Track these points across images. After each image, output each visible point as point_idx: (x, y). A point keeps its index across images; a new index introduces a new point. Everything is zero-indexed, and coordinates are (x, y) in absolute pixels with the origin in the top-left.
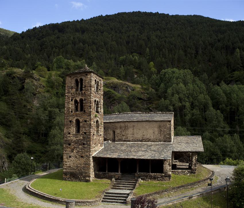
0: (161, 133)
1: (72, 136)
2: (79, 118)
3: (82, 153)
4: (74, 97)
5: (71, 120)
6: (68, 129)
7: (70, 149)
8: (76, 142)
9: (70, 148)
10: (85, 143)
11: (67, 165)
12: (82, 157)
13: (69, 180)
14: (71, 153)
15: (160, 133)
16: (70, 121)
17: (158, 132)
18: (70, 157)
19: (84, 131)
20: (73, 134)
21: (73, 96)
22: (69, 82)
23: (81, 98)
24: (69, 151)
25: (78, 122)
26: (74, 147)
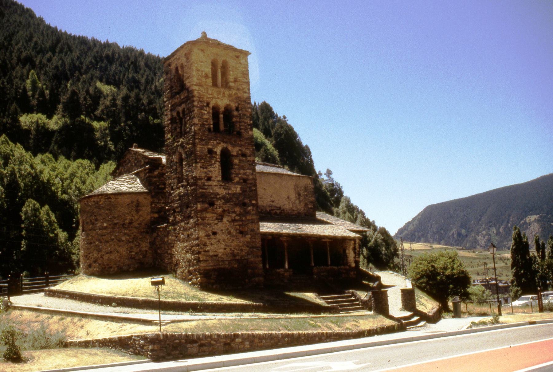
0: (299, 199)
1: (216, 186)
2: (230, 148)
3: (241, 223)
4: (213, 98)
5: (210, 147)
6: (206, 168)
7: (213, 215)
8: (227, 200)
10: (247, 201)
11: (208, 251)
12: (241, 232)
14: (216, 224)
15: (299, 199)
17: (296, 197)
18: (215, 233)
20: (218, 181)
21: (210, 94)
23: (228, 102)
24: (211, 219)
25: (226, 156)
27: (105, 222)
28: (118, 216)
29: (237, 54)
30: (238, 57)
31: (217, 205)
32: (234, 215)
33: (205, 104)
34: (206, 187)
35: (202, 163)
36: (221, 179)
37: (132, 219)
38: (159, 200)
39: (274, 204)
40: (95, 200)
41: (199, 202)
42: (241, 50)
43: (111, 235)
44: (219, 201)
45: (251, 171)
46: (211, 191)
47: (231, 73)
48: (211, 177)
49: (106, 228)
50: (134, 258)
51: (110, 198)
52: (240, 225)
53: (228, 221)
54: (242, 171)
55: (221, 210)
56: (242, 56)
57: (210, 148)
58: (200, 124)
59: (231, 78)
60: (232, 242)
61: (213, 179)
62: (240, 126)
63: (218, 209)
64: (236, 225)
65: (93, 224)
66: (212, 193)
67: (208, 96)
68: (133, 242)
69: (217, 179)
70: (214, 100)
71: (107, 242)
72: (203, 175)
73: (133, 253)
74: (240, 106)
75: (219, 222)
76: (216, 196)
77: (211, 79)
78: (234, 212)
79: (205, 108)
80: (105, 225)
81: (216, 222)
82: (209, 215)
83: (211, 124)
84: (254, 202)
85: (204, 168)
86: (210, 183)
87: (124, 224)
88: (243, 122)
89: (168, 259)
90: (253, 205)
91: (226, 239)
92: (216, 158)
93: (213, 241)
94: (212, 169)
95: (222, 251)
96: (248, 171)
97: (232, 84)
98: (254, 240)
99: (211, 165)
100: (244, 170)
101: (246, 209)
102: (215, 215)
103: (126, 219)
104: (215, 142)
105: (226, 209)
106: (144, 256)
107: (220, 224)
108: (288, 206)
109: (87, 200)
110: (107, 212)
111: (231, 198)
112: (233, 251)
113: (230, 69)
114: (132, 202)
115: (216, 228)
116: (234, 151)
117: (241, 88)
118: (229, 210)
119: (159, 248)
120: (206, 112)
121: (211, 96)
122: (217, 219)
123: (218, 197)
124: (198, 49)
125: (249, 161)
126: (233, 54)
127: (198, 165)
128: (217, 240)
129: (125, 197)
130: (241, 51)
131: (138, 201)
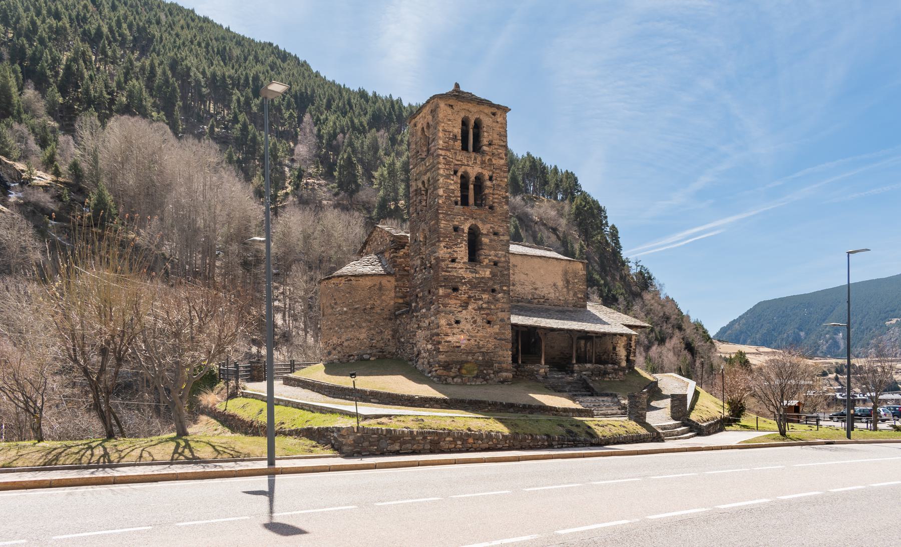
0: (568, 286)
2: (480, 225)
3: (489, 312)
4: (462, 165)
6: (451, 248)
8: (473, 285)
9: (456, 298)
10: (497, 287)
12: (489, 322)
13: (457, 384)
14: (459, 312)
15: (567, 287)
16: (456, 229)
17: (564, 285)
18: (457, 322)
19: (494, 258)
20: (464, 263)
22: (449, 120)
23: (480, 170)
24: (454, 306)
26: (468, 298)
27: (345, 307)
28: (358, 301)
29: (494, 110)
30: (494, 114)
31: (461, 290)
32: (481, 302)
33: (452, 173)
34: (450, 270)
35: (446, 241)
36: (467, 261)
37: (374, 304)
38: (404, 284)
39: (537, 292)
40: (335, 282)
41: (441, 286)
42: (498, 105)
43: (351, 321)
44: (464, 286)
45: (504, 253)
46: (455, 274)
47: (485, 134)
48: (457, 258)
49: (346, 312)
50: (375, 346)
51: (351, 280)
52: (487, 314)
53: (473, 309)
54: (492, 253)
55: (466, 296)
56: (499, 113)
57: (455, 225)
58: (446, 196)
59: (485, 141)
60: (477, 333)
61: (457, 260)
62: (493, 198)
63: (463, 295)
64: (483, 314)
65: (333, 308)
66: (458, 277)
67: (457, 163)
68: (374, 329)
69: (462, 261)
70: (463, 167)
71: (347, 328)
72: (448, 256)
73: (374, 341)
74: (494, 175)
75: (463, 309)
76: (462, 280)
77: (460, 141)
78: (481, 299)
79: (452, 177)
80: (345, 309)
81: (460, 309)
82: (452, 302)
83: (458, 197)
84: (505, 288)
85: (447, 248)
86: (455, 265)
87: (365, 309)
88: (497, 194)
89: (410, 349)
90: (504, 292)
91: (471, 328)
92: (462, 236)
93: (455, 331)
94: (456, 249)
95: (465, 342)
96: (500, 252)
97: (485, 148)
98: (503, 331)
99: (456, 245)
100: (495, 250)
101: (495, 296)
102: (459, 302)
103: (368, 304)
104: (462, 218)
105: (473, 295)
106: (386, 345)
107: (464, 312)
108: (553, 294)
109: (327, 281)
110: (347, 295)
111: (479, 283)
112: (479, 342)
113: (485, 129)
114: (375, 285)
115: (460, 316)
116: (484, 228)
117: (496, 153)
118: (475, 296)
119: (401, 337)
120: (452, 182)
121: (459, 163)
122: (460, 306)
123: (463, 281)
124: (446, 105)
125: (501, 240)
126: (488, 110)
127: (441, 245)
128: (460, 330)
129: (367, 279)
130: (498, 107)
131: (380, 283)
